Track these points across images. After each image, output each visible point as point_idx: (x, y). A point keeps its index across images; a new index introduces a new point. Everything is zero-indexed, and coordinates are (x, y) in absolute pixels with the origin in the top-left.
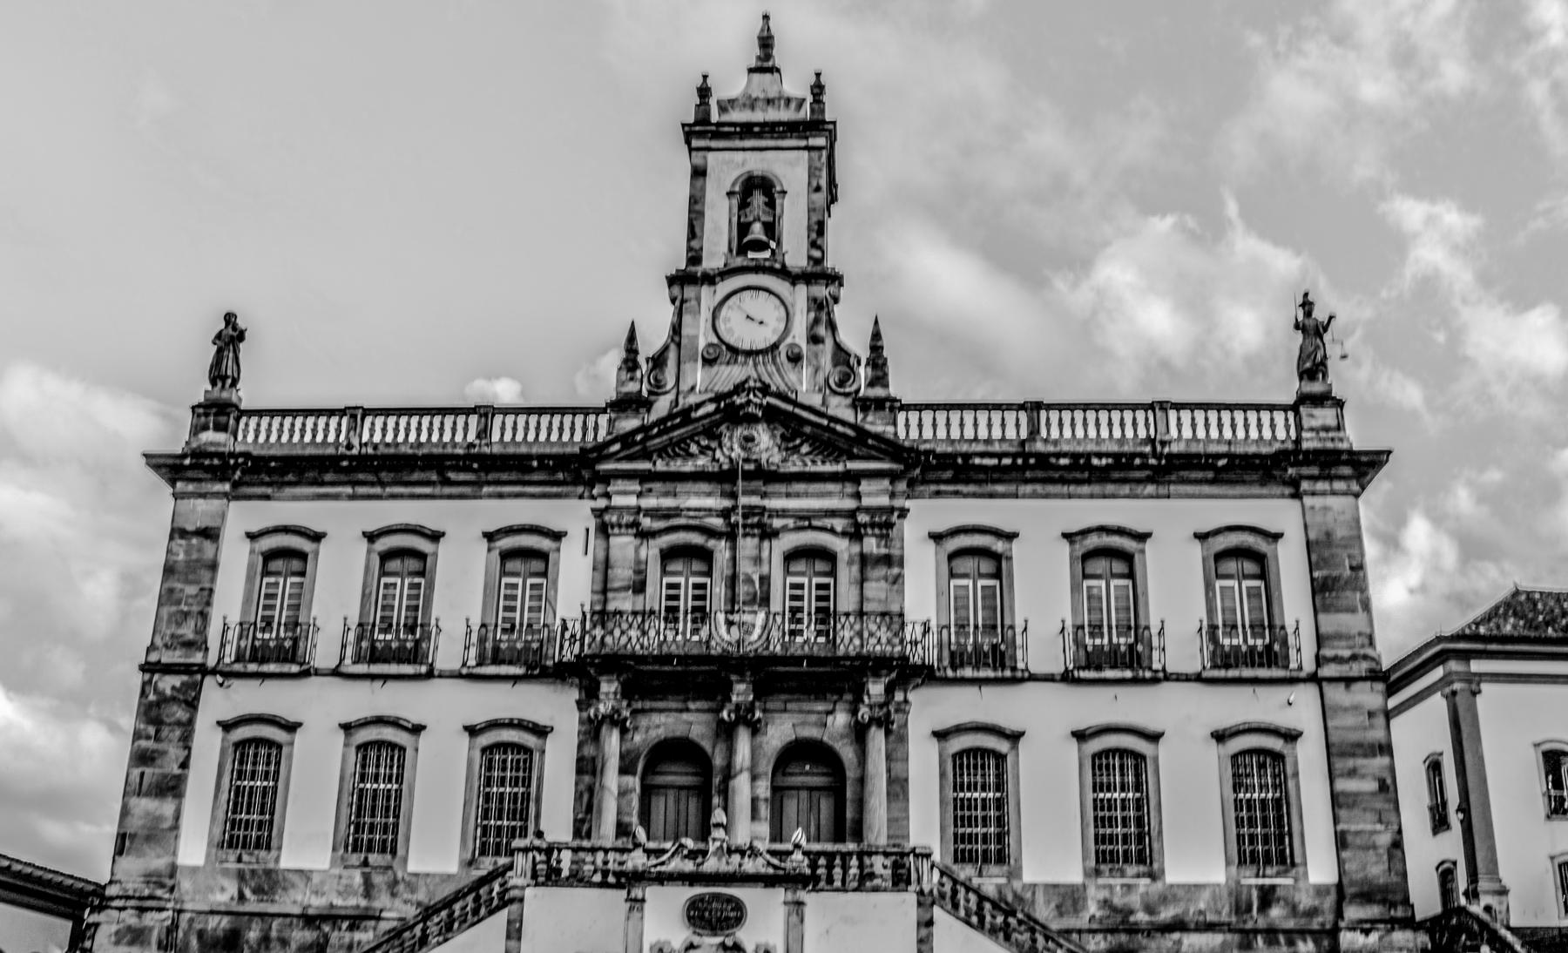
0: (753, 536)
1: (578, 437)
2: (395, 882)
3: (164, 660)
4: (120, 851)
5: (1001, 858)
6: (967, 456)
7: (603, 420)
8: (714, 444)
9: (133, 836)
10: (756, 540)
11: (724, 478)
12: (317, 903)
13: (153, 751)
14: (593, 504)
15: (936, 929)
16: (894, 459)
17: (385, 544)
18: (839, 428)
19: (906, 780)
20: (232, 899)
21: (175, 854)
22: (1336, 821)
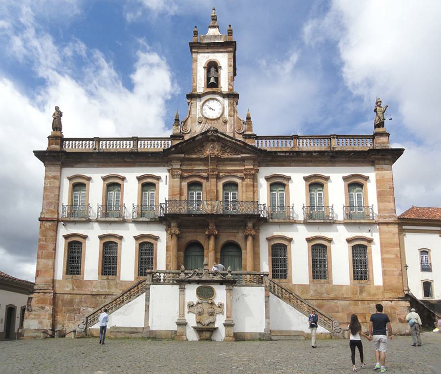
0: (214, 178)
1: (163, 147)
2: (117, 284)
3: (46, 217)
4: (37, 275)
5: (285, 277)
6: (276, 152)
7: (170, 142)
8: (202, 149)
9: (41, 271)
10: (215, 179)
11: (205, 160)
12: (95, 291)
13: (45, 245)
14: (168, 168)
15: (270, 298)
16: (255, 153)
17: (107, 182)
18: (238, 143)
19: (259, 253)
20: (71, 290)
21: (54, 276)
22: (383, 267)
